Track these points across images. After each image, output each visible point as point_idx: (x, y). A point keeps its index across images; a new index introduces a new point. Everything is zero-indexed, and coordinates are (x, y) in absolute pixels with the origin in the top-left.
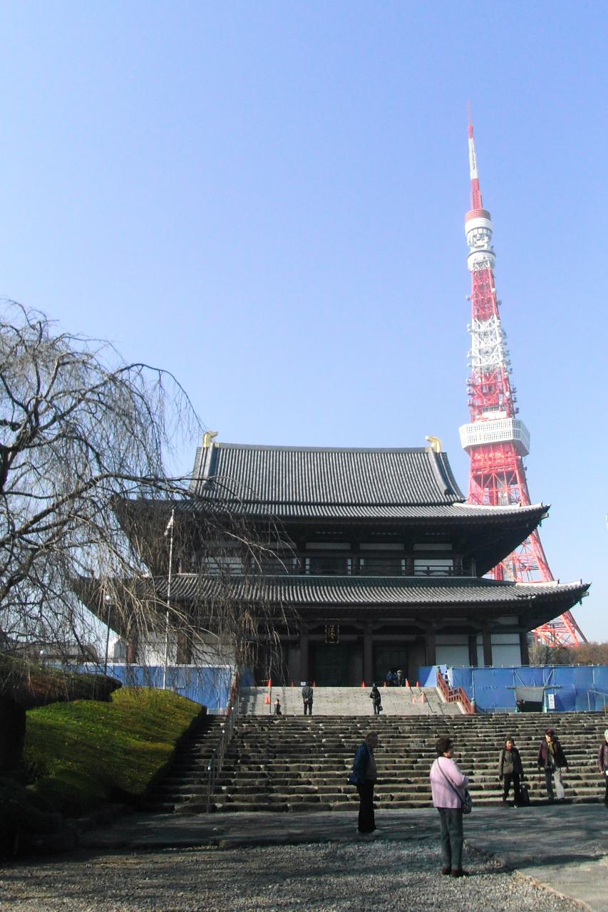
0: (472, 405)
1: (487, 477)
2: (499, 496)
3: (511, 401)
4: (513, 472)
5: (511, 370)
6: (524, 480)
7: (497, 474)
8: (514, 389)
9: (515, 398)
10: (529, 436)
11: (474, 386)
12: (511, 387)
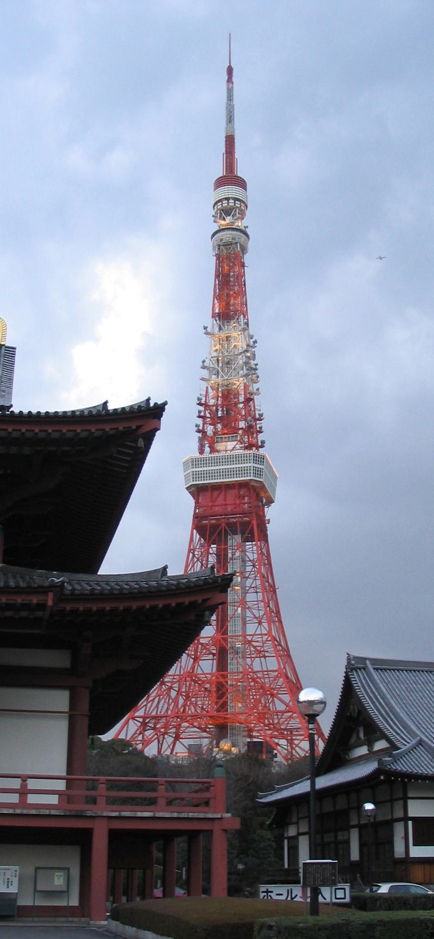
0: (203, 432)
1: (214, 528)
2: (230, 555)
3: (251, 430)
4: (249, 523)
5: (258, 390)
6: (264, 537)
7: (228, 524)
8: (261, 415)
9: (261, 428)
10: (275, 478)
11: (206, 405)
12: (257, 413)
